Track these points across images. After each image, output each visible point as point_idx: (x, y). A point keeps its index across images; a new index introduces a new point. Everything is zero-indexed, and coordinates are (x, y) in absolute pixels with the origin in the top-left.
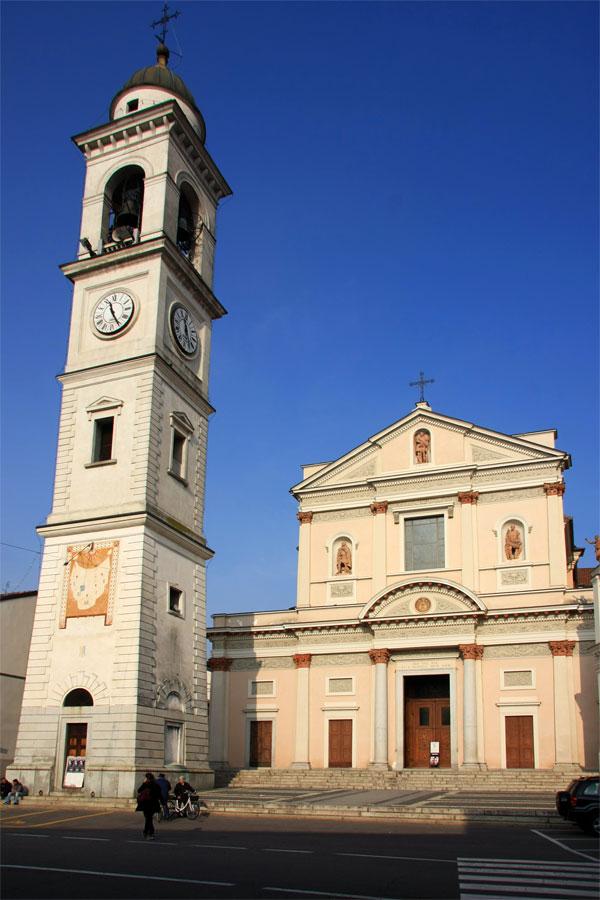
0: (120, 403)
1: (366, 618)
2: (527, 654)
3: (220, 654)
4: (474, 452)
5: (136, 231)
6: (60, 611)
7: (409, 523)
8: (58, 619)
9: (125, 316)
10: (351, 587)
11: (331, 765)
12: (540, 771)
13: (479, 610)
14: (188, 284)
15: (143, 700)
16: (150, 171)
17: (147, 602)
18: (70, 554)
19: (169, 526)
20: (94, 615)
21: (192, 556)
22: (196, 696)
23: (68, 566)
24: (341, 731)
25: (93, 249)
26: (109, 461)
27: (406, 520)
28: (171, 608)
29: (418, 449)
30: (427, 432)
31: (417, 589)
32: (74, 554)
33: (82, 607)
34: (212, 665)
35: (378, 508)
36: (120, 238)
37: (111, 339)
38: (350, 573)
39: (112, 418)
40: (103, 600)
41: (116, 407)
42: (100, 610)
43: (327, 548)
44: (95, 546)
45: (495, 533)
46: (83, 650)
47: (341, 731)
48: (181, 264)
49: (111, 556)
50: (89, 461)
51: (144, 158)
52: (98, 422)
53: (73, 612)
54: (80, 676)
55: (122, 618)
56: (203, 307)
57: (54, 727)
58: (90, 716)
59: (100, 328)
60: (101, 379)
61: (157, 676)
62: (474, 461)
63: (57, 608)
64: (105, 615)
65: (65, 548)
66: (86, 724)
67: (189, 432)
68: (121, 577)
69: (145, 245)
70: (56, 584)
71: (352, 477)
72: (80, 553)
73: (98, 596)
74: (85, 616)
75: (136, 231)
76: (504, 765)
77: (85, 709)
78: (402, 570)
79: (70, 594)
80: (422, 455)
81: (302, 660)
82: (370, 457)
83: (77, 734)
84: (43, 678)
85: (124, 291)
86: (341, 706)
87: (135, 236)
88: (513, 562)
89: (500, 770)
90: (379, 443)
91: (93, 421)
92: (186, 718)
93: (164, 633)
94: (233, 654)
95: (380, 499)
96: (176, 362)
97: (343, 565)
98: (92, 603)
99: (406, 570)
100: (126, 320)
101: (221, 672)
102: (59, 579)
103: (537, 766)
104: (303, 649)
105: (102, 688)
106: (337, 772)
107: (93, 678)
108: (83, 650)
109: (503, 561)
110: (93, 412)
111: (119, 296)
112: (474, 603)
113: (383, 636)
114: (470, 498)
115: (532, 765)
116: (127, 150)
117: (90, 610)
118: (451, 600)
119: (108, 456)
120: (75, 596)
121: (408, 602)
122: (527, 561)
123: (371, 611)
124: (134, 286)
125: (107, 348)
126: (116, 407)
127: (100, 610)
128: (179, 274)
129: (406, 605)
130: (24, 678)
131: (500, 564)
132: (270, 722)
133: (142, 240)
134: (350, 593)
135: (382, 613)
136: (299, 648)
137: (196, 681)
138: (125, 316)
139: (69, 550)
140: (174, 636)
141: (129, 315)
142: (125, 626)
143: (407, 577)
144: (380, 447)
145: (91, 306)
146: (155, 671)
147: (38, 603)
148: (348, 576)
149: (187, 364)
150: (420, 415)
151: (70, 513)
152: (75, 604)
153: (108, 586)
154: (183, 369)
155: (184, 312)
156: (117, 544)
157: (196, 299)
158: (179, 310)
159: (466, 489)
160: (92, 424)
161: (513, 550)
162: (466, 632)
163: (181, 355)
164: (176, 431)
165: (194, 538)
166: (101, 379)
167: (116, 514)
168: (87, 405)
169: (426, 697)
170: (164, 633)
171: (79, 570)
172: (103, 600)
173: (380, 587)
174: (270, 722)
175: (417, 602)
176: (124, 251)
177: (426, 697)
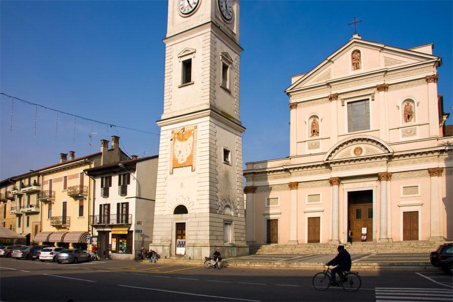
0: (194, 51)
1: (327, 160)
2: (415, 177)
3: (250, 184)
6: (169, 165)
7: (350, 105)
9: (195, 3)
11: (309, 241)
12: (422, 241)
13: (389, 152)
15: (212, 210)
18: (173, 135)
19: (221, 115)
22: (238, 207)
23: (173, 141)
24: (314, 224)
26: (190, 83)
28: (225, 160)
29: (354, 62)
30: (359, 52)
31: (355, 142)
33: (180, 162)
34: (247, 190)
38: (318, 135)
39: (191, 59)
40: (190, 158)
41: (192, 53)
42: (189, 163)
43: (305, 122)
44: (185, 130)
45: (398, 107)
46: (182, 185)
47: (314, 224)
49: (193, 134)
50: (180, 84)
53: (176, 166)
57: (170, 225)
58: (186, 219)
60: (184, 39)
61: (219, 197)
62: (386, 65)
65: (170, 131)
66: (185, 223)
67: (230, 63)
68: (199, 145)
71: (318, 81)
72: (178, 134)
74: (182, 167)
76: (402, 239)
77: (184, 215)
78: (347, 132)
79: (174, 155)
80: (356, 65)
81: (293, 186)
83: (181, 228)
84: (164, 200)
86: (313, 210)
89: (400, 242)
91: (181, 62)
92: (234, 218)
94: (257, 184)
95: (334, 92)
96: (221, 24)
97: (314, 131)
98: (185, 160)
99: (349, 132)
100: (195, 5)
101: (251, 194)
103: (420, 239)
104: (294, 179)
105: (192, 204)
106: (312, 245)
107: (187, 199)
108: (182, 185)
110: (181, 57)
112: (386, 149)
114: (383, 88)
115: (417, 239)
117: (184, 163)
121: (350, 150)
122: (417, 123)
123: (330, 156)
125: (187, 21)
126: (192, 53)
127: (189, 163)
129: (349, 152)
130: (154, 201)
131: (401, 125)
132: (277, 220)
134: (318, 147)
136: (292, 179)
137: (238, 199)
138: (195, 3)
140: (227, 175)
144: (333, 62)
146: (218, 194)
147: (159, 162)
150: (355, 42)
153: (192, 150)
156: (196, 127)
159: (381, 83)
160: (181, 64)
161: (409, 117)
162: (382, 165)
163: (224, 21)
164: (223, 62)
165: (235, 121)
166: (184, 39)
167: (195, 111)
169: (360, 202)
171: (178, 143)
172: (190, 158)
173: (335, 142)
174: (277, 220)
177: (360, 202)
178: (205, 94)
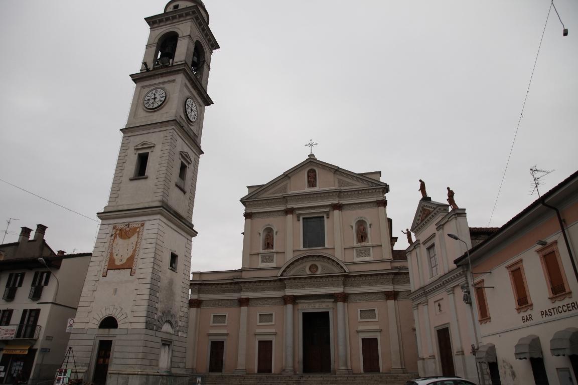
0: (153, 145)
1: (281, 275)
2: (372, 299)
3: (195, 297)
4: (339, 181)
5: (171, 60)
6: (104, 265)
7: (305, 220)
8: (102, 271)
9: (161, 101)
10: (273, 257)
11: (260, 371)
12: (383, 373)
13: (345, 272)
14: (195, 87)
15: (149, 325)
16: (181, 34)
17: (156, 261)
18: (115, 230)
19: (174, 216)
20: (124, 269)
21: (185, 234)
22: (180, 324)
23: (113, 238)
24: (265, 348)
25: (148, 67)
26: (144, 177)
27: (303, 219)
28: (171, 266)
29: (310, 180)
30: (314, 171)
31: (310, 259)
32: (117, 230)
33: (118, 263)
34: (193, 304)
35: (288, 211)
36: (162, 63)
37: (152, 112)
38: (273, 249)
39: (148, 153)
40: (131, 259)
41: (151, 147)
42: (129, 265)
43: (260, 234)
44: (130, 226)
45: (352, 227)
46: (116, 291)
47: (265, 348)
48: (193, 77)
49: (139, 232)
50: (132, 175)
51: (179, 29)
52: (139, 155)
53: (112, 266)
54: (112, 308)
55: (142, 271)
56: (201, 99)
57: (91, 343)
58: (114, 336)
59: (147, 106)
60: (144, 132)
61: (159, 309)
62: (339, 187)
63: (103, 264)
64: (131, 268)
65: (112, 226)
66: (112, 341)
67: (189, 163)
68: (144, 244)
69: (175, 67)
70: (106, 239)
71: (274, 194)
72: (121, 230)
73: (128, 257)
74: (119, 269)
75: (171, 60)
76: (362, 370)
77: (113, 331)
78: (302, 247)
79: (112, 254)
80: (312, 183)
81: (243, 302)
82: (282, 184)
83: (105, 347)
84: (89, 309)
85: (161, 88)
87: (171, 62)
88: (363, 244)
89: (361, 374)
90: (289, 175)
91: (137, 154)
92: (174, 338)
93: (164, 282)
95: (289, 206)
96: (184, 124)
97: (268, 244)
98: (124, 261)
100: (161, 103)
101: (195, 309)
102: (107, 245)
103: (381, 370)
104: (244, 295)
105: (124, 316)
106: (264, 375)
107: (119, 310)
108: (116, 291)
109: (357, 243)
110: (137, 149)
111: (159, 90)
112: (342, 267)
113: (291, 287)
114: (338, 207)
115: (378, 371)
116: (171, 25)
117: (122, 265)
118: (329, 266)
119: (144, 174)
120: (115, 256)
121: (305, 266)
122: (370, 244)
123: (284, 271)
124: (167, 87)
125: (149, 116)
126: (151, 147)
127: (129, 265)
128: (191, 82)
129: (305, 269)
130: (77, 309)
131: (355, 244)
132: (223, 342)
133: (174, 64)
134: (272, 261)
135: (291, 273)
136: (242, 294)
137: (181, 314)
138: (161, 101)
139: (114, 228)
140: (171, 283)
141: (163, 100)
142: (142, 276)
143: (305, 252)
144: (290, 178)
145: (143, 96)
146: (157, 306)
147: (92, 260)
148: (272, 250)
149: (191, 127)
150: (311, 161)
151: (118, 206)
152: (114, 260)
153: (135, 251)
154: (188, 129)
155: (192, 101)
156: (143, 225)
157: (198, 95)
158: (189, 100)
159: (336, 202)
160: (137, 155)
161: (362, 237)
162: (338, 285)
163: (188, 122)
164: (182, 161)
165: (187, 224)
166: (144, 132)
167: (144, 207)
168: (135, 145)
169: (316, 327)
170: (164, 282)
171: (119, 241)
172: (131, 259)
173: (290, 257)
174: (223, 342)
175: (310, 269)
176: (164, 69)
177: (316, 327)
178: (158, 191)
